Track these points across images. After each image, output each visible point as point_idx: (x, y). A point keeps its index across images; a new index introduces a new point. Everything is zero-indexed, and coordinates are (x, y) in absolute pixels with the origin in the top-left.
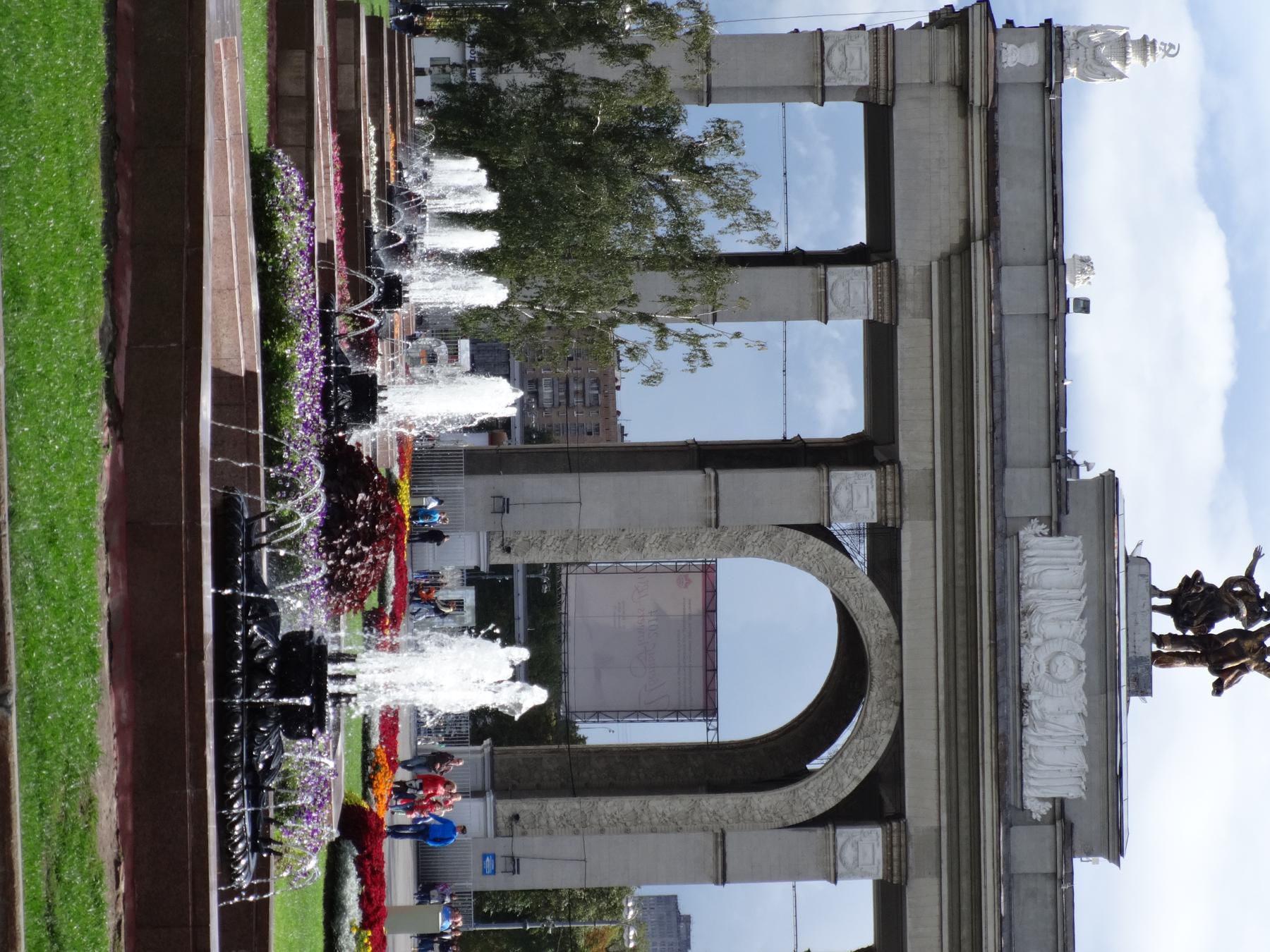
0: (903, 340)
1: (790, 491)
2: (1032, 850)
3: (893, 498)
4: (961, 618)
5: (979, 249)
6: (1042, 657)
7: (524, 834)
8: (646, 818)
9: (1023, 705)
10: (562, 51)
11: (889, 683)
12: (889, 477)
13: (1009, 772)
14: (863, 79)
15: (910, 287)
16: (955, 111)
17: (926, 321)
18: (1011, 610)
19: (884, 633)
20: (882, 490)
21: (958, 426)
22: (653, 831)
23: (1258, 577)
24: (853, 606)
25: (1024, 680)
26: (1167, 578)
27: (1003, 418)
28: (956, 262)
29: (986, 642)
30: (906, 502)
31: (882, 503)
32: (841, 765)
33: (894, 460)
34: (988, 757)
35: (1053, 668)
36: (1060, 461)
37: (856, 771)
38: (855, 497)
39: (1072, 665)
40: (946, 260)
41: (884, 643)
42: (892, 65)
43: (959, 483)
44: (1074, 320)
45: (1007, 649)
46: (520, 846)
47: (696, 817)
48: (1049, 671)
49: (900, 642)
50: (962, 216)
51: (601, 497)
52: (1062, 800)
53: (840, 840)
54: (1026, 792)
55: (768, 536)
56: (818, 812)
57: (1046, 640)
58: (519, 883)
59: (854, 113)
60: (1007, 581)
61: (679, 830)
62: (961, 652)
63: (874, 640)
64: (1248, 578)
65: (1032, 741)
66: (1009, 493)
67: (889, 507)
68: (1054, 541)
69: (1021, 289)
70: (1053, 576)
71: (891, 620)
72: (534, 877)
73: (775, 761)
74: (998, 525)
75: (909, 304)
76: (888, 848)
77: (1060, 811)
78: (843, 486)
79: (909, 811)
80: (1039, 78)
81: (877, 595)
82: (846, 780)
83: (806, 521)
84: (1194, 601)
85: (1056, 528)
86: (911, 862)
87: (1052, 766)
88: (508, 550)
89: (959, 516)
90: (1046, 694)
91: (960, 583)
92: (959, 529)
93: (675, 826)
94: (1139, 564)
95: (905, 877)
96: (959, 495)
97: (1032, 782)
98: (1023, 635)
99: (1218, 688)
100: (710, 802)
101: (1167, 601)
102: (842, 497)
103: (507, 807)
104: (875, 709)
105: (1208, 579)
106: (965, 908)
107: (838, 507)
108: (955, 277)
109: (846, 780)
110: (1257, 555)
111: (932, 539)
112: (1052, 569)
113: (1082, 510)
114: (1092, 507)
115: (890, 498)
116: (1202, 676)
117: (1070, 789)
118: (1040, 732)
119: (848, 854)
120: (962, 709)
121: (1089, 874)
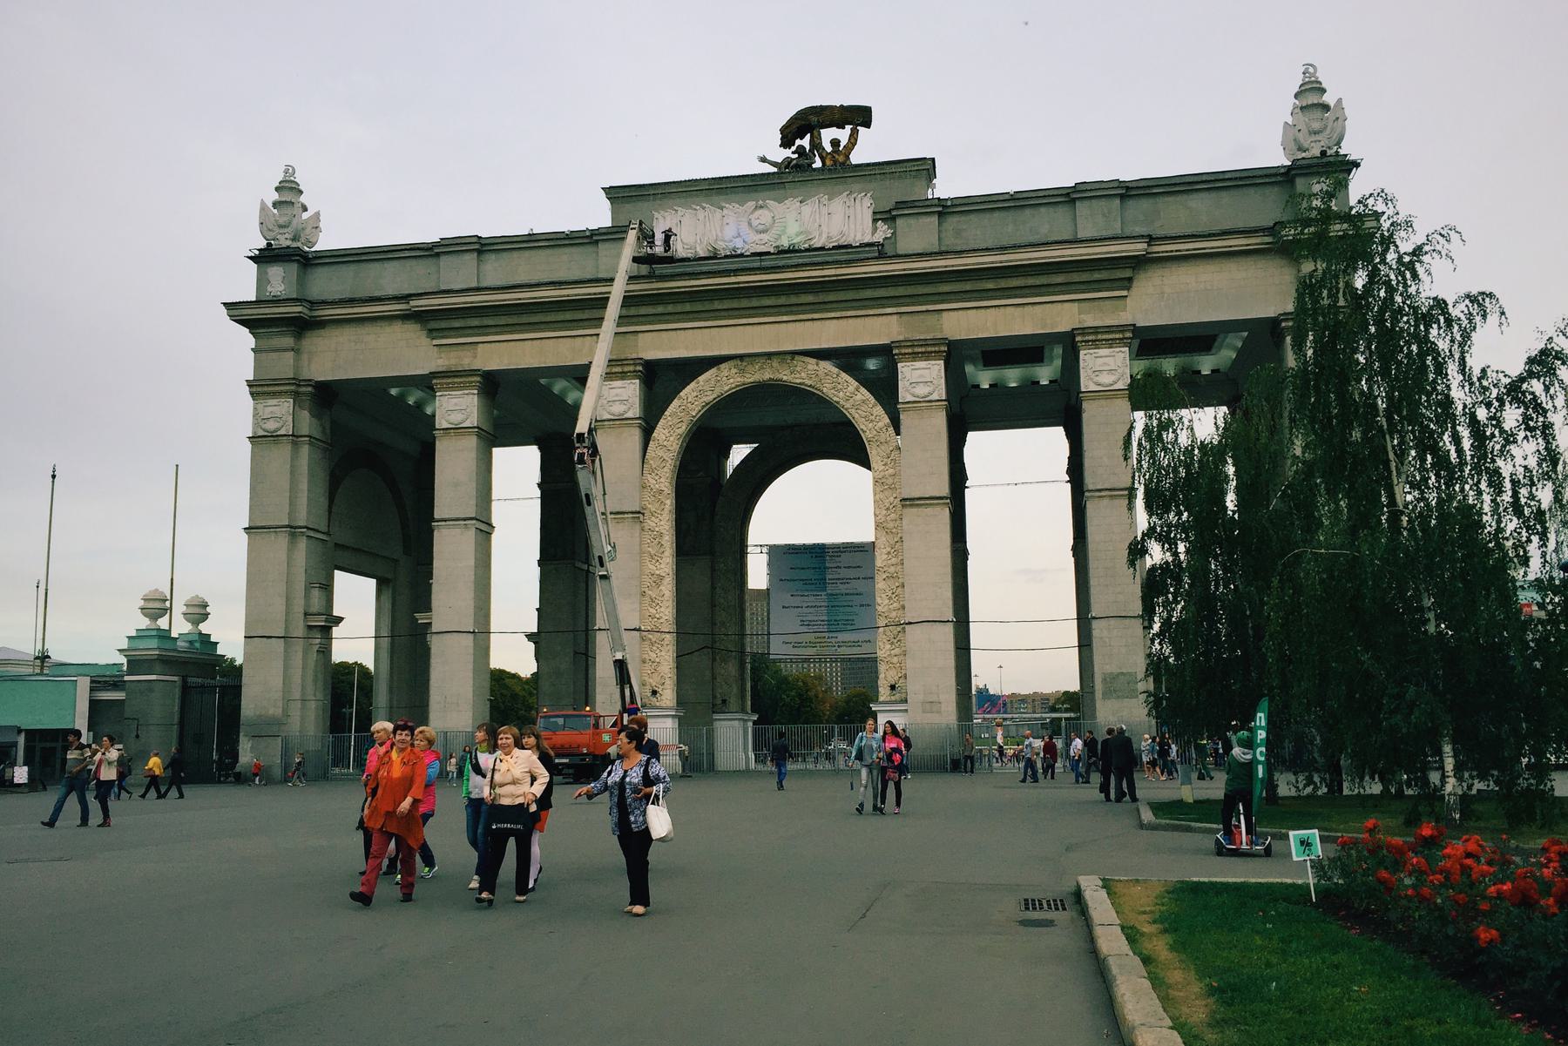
2: (917, 235)
4: (717, 305)
8: (892, 569)
9: (791, 251)
13: (845, 252)
15: (453, 362)
16: (322, 332)
19: (734, 371)
29: (733, 279)
40: (432, 333)
41: (742, 371)
47: (891, 525)
67: (626, 369)
69: (458, 273)
71: (723, 366)
75: (467, 360)
76: (915, 356)
79: (886, 341)
80: (295, 266)
82: (859, 397)
87: (842, 219)
90: (784, 232)
109: (859, 397)
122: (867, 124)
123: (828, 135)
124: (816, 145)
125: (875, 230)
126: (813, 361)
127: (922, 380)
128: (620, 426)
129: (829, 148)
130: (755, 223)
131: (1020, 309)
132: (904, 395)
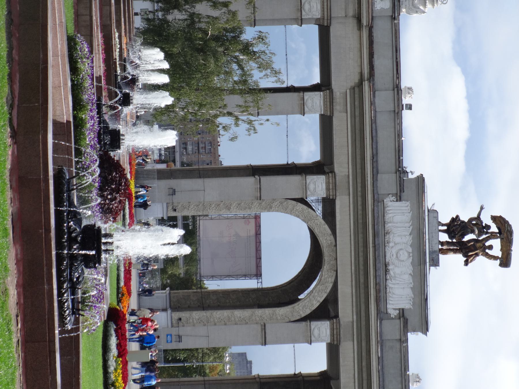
0: (336, 122)
1: (290, 184)
2: (391, 329)
3: (332, 187)
4: (361, 236)
5: (366, 84)
6: (394, 251)
7: (183, 326)
8: (233, 319)
9: (386, 271)
10: (194, 5)
11: (332, 262)
12: (330, 178)
14: (318, 15)
15: (338, 100)
17: (345, 114)
18: (381, 233)
19: (329, 242)
20: (328, 184)
21: (358, 157)
22: (236, 324)
23: (482, 217)
24: (316, 231)
25: (387, 261)
26: (445, 218)
27: (377, 154)
28: (357, 90)
29: (371, 245)
30: (337, 188)
31: (328, 189)
32: (312, 297)
33: (332, 172)
34: (372, 292)
35: (399, 255)
36: (400, 171)
37: (319, 299)
38: (317, 186)
39: (406, 254)
40: (353, 89)
42: (330, 9)
43: (359, 180)
44: (405, 113)
45: (380, 247)
46: (182, 331)
47: (254, 318)
48: (397, 257)
49: (336, 246)
50: (359, 71)
51: (213, 188)
52: (403, 309)
53: (312, 327)
54: (388, 306)
55: (281, 203)
56: (303, 315)
57: (395, 244)
58: (181, 346)
59: (315, 29)
60: (380, 219)
61: (247, 323)
62: (361, 249)
63: (325, 245)
64: (478, 218)
65: (390, 285)
66: (379, 184)
67: (331, 191)
68: (398, 203)
69: (384, 100)
70: (398, 218)
71: (332, 237)
72: (187, 343)
73: (285, 295)
74: (376, 197)
75: (338, 107)
76: (332, 329)
77: (402, 314)
79: (340, 315)
80: (390, 14)
81: (326, 227)
82: (315, 302)
83: (297, 197)
84: (456, 227)
85: (399, 199)
86: (341, 335)
87: (399, 295)
88: (175, 210)
89: (359, 194)
90: (396, 266)
91: (360, 221)
92: (360, 199)
93: (245, 322)
94: (434, 213)
95: (339, 341)
96: (359, 185)
97: (391, 302)
98: (386, 242)
99: (466, 263)
100: (259, 312)
101: (445, 228)
102: (311, 187)
103: (177, 315)
104: (326, 273)
105: (462, 218)
106: (364, 354)
107: (310, 191)
108: (357, 96)
109: (315, 302)
110: (482, 208)
111: (348, 204)
112: (397, 215)
113: (410, 191)
114: (414, 189)
115: (331, 187)
116: (460, 258)
117: (406, 304)
118: (394, 282)
119: (316, 332)
120: (362, 273)
121: (414, 339)
122: (501, 265)
123: (496, 244)
124: (493, 236)
125: (395, 309)
129: (487, 244)
130: (401, 252)
131: (352, 376)
132: (315, 324)
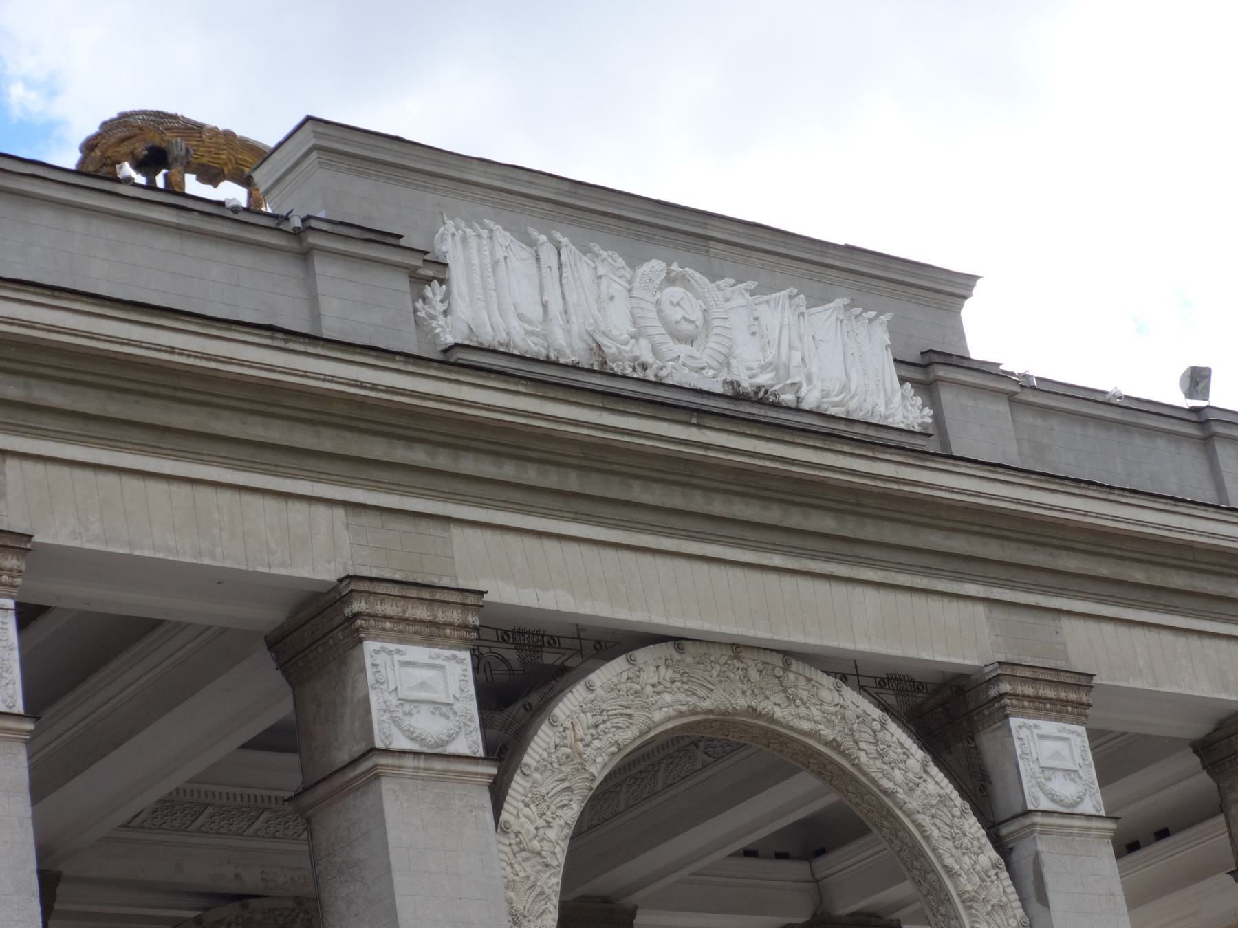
12: (379, 608)
19: (666, 674)
25: (719, 389)
31: (431, 633)
38: (423, 695)
39: (676, 292)
48: (691, 341)
63: (682, 697)
67: (442, 615)
68: (457, 274)
78: (407, 721)
98: (639, 374)
104: (802, 711)
107: (451, 738)
109: (931, 787)
111: (488, 535)
115: (422, 613)
126: (828, 681)
127: (1050, 759)
128: (443, 777)
